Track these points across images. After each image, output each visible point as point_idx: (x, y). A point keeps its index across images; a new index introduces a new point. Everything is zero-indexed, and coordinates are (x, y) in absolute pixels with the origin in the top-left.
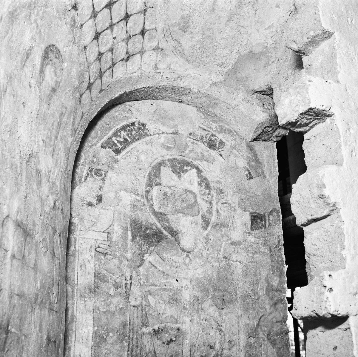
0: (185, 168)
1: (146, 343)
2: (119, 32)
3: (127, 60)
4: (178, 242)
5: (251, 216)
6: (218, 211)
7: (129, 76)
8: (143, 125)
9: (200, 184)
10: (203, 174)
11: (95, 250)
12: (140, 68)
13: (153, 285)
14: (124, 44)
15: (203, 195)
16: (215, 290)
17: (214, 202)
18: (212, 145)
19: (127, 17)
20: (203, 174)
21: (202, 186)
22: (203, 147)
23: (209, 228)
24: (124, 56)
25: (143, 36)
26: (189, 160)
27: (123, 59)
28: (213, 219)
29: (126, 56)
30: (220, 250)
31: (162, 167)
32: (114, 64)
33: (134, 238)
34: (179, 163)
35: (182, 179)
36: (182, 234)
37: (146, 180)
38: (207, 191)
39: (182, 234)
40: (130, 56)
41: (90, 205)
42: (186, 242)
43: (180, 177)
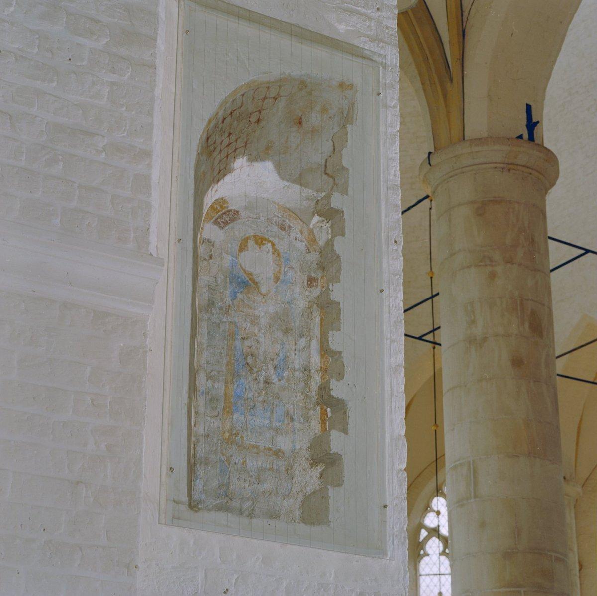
0: (264, 242)
1: (237, 344)
4: (258, 287)
5: (308, 278)
6: (285, 272)
8: (237, 212)
9: (273, 253)
10: (275, 247)
11: (209, 287)
13: (242, 312)
15: (275, 260)
16: (281, 321)
17: (283, 266)
18: (283, 228)
20: (275, 247)
21: (274, 255)
22: (276, 229)
23: (279, 282)
26: (267, 237)
28: (281, 277)
30: (285, 297)
31: (249, 241)
33: (231, 282)
34: (260, 239)
35: (261, 249)
36: (260, 284)
37: (238, 248)
38: (278, 258)
39: (260, 284)
41: (205, 259)
42: (264, 290)
43: (260, 248)
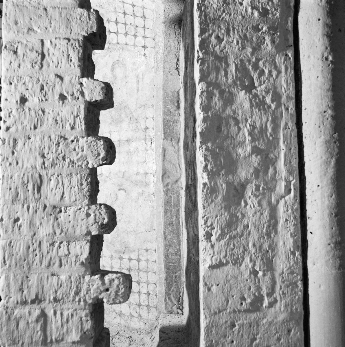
2: (130, 19)
3: (146, 18)
7: (155, 18)
12: (152, 11)
14: (136, 18)
19: (125, 14)
24: (142, 20)
25: (135, 6)
27: (144, 20)
29: (143, 18)
32: (144, 27)
40: (144, 16)
